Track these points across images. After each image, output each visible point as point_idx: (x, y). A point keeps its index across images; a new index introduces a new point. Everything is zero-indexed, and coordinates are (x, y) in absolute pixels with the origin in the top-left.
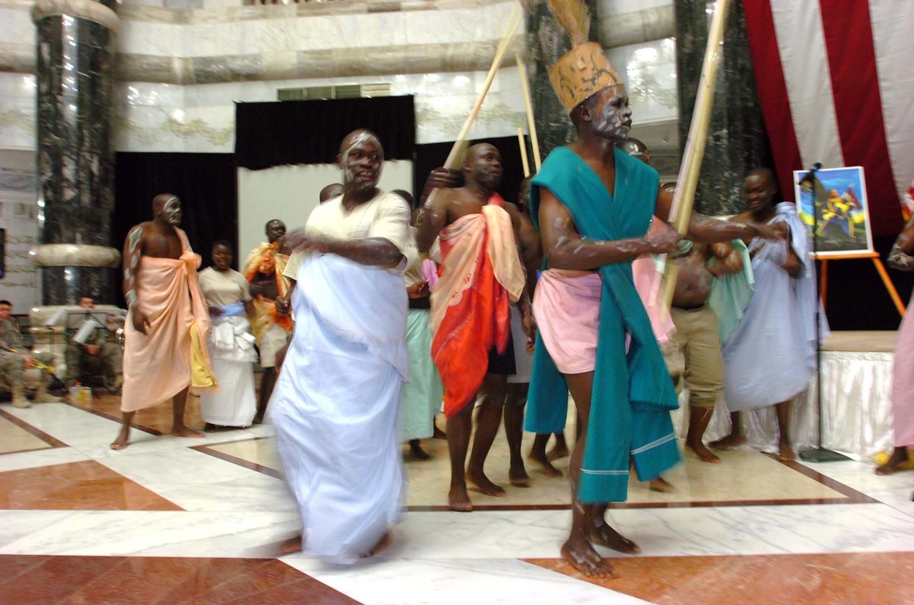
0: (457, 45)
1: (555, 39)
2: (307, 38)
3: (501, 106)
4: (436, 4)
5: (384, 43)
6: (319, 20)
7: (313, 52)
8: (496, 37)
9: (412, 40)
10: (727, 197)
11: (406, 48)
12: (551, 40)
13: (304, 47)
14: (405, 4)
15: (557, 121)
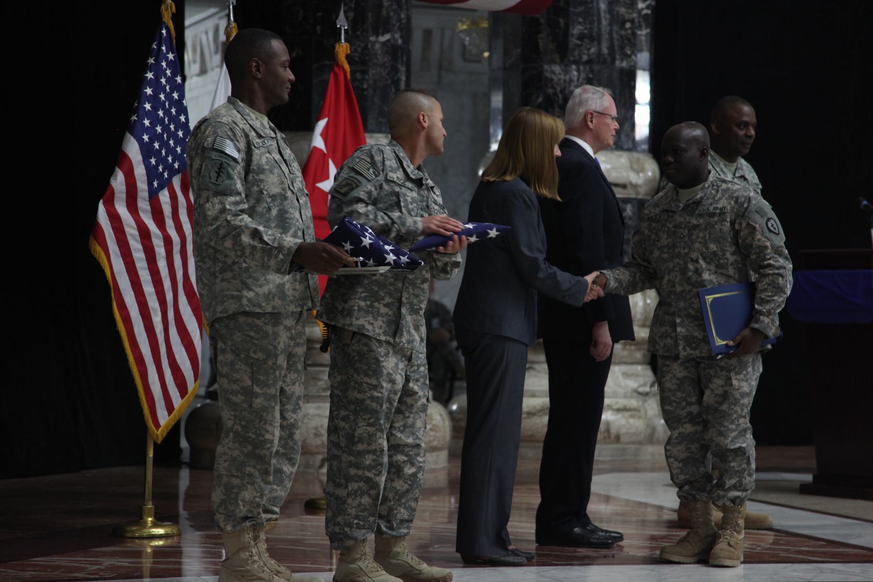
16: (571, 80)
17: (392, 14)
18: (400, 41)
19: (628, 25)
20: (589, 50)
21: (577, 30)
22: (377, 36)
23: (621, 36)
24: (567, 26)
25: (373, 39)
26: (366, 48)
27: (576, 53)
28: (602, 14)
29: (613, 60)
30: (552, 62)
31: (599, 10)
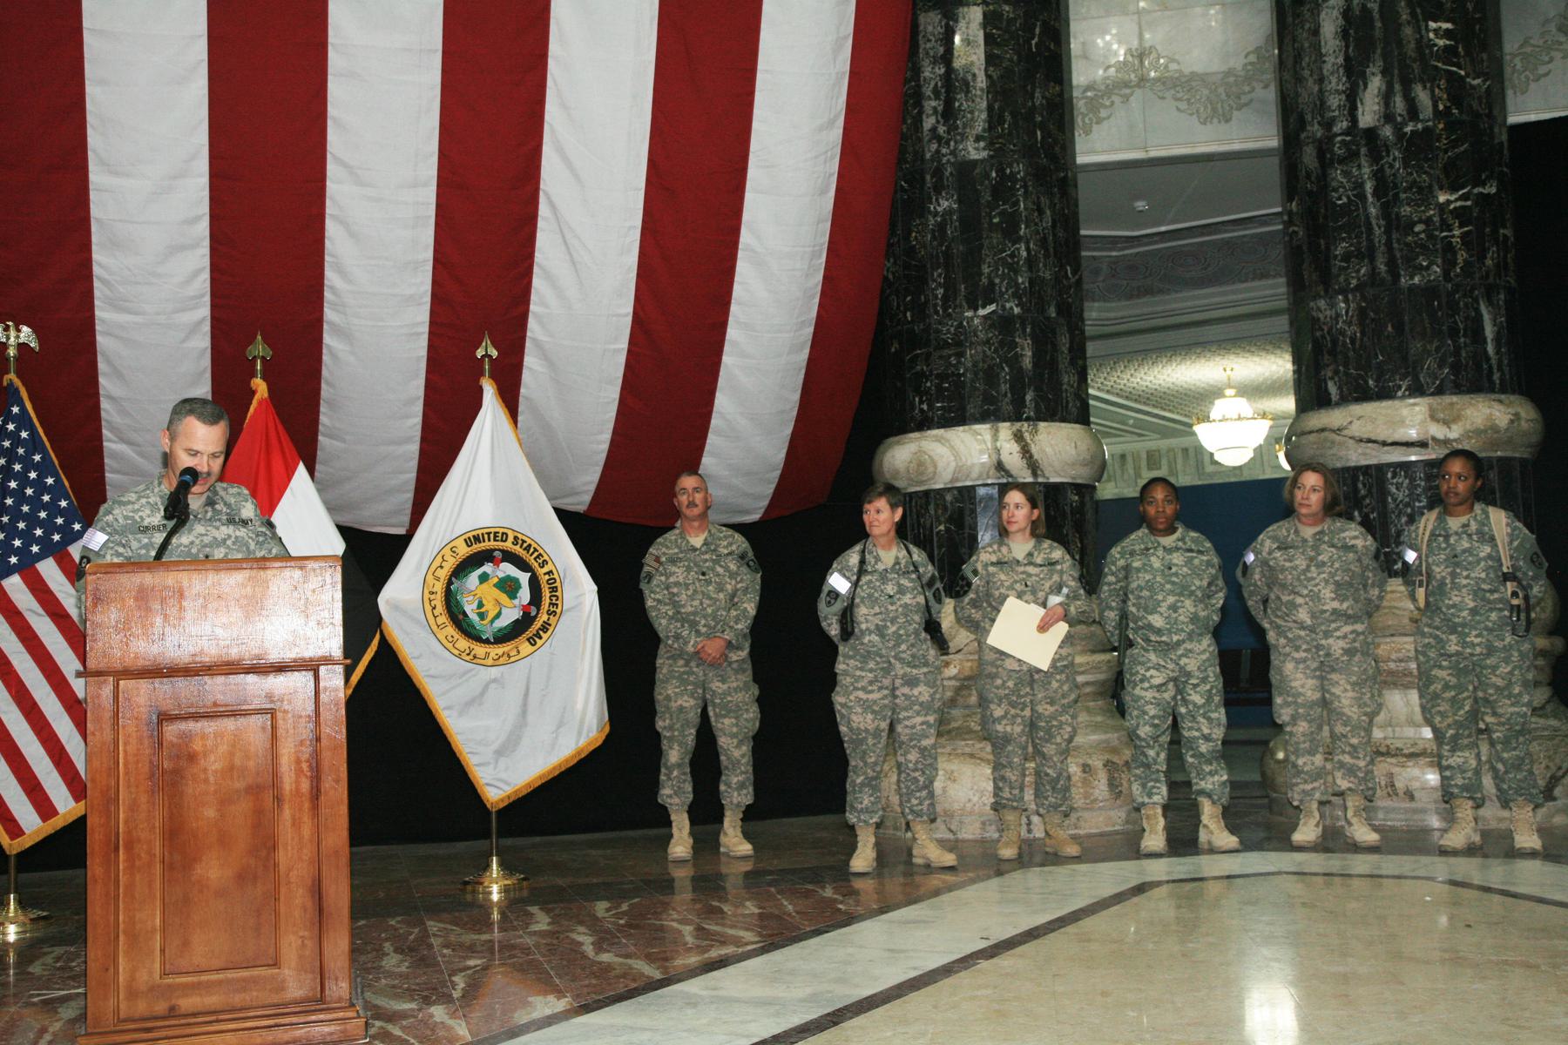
16: (1338, 315)
17: (997, 281)
18: (1017, 310)
19: (1418, 228)
20: (1358, 271)
21: (1340, 249)
22: (976, 309)
23: (1407, 245)
24: (1328, 249)
25: (969, 314)
26: (960, 325)
27: (1342, 279)
28: (1374, 222)
29: (1396, 277)
30: (1316, 297)
31: (1367, 217)
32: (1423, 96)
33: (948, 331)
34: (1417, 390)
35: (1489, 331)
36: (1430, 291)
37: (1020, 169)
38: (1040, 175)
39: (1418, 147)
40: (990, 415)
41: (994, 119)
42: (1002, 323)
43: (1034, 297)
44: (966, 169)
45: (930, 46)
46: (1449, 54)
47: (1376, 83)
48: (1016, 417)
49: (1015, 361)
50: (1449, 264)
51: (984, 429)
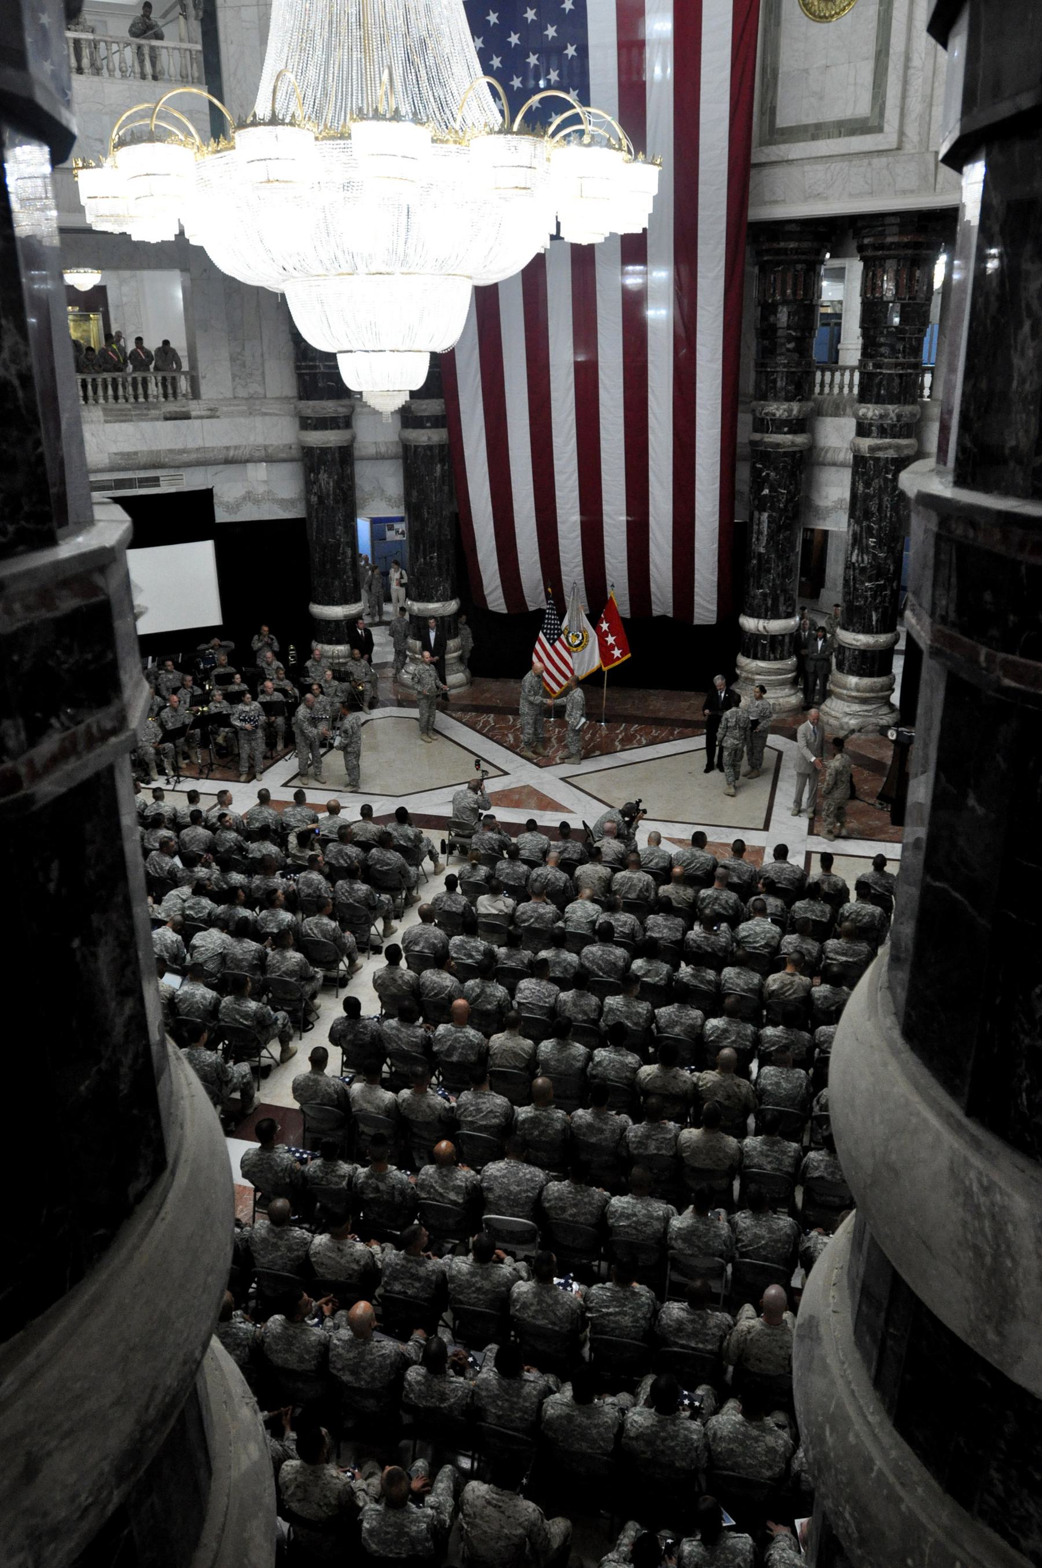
0: (236, 448)
1: (331, 484)
2: (115, 442)
3: (269, 492)
4: (218, 414)
5: (179, 446)
6: (124, 425)
7: (122, 454)
8: (266, 443)
9: (199, 443)
10: (437, 591)
11: (198, 450)
12: (328, 483)
13: (114, 449)
14: (193, 414)
15: (334, 538)
32: (866, 558)
33: (752, 593)
34: (854, 631)
35: (874, 618)
36: (859, 608)
37: (773, 556)
38: (779, 557)
39: (863, 570)
40: (759, 617)
41: (768, 542)
42: (764, 595)
43: (774, 588)
44: (760, 554)
45: (756, 520)
46: (874, 547)
47: (856, 551)
48: (765, 618)
49: (766, 605)
50: (866, 601)
51: (756, 620)
